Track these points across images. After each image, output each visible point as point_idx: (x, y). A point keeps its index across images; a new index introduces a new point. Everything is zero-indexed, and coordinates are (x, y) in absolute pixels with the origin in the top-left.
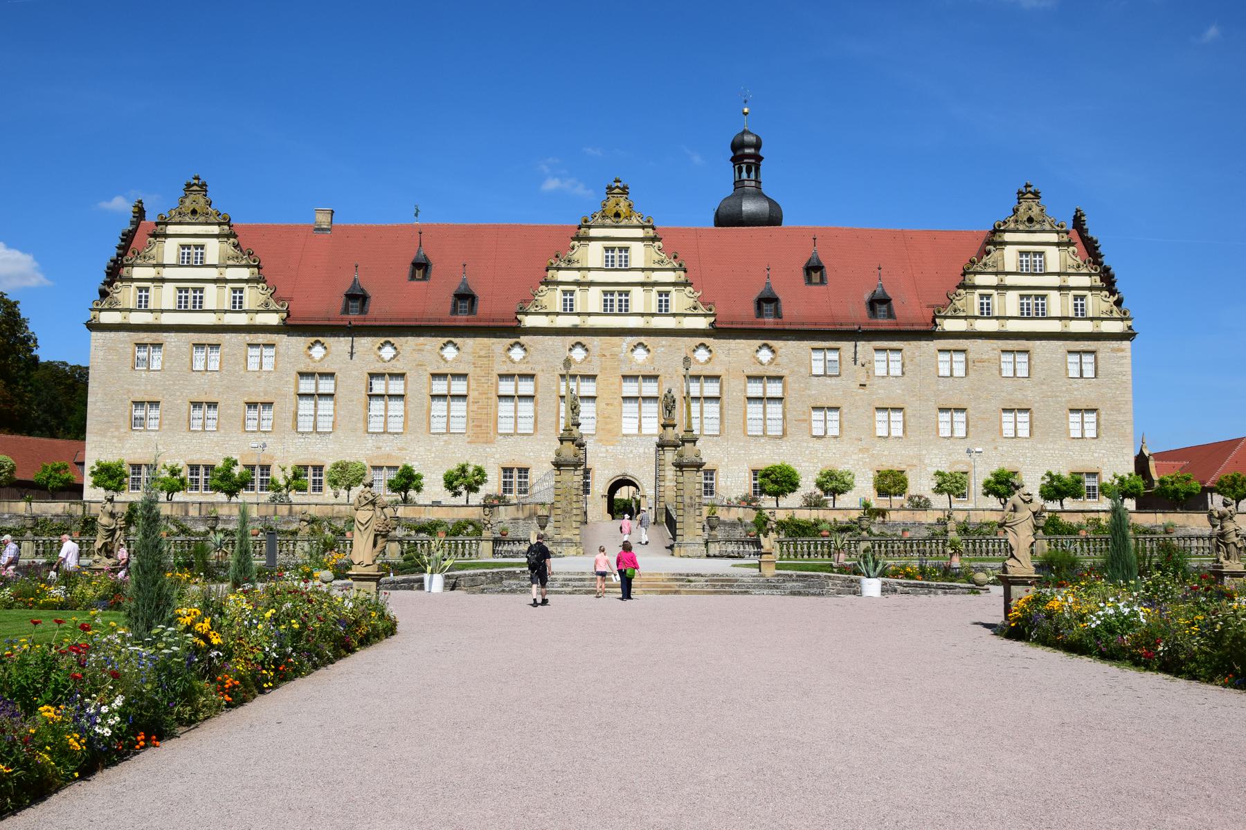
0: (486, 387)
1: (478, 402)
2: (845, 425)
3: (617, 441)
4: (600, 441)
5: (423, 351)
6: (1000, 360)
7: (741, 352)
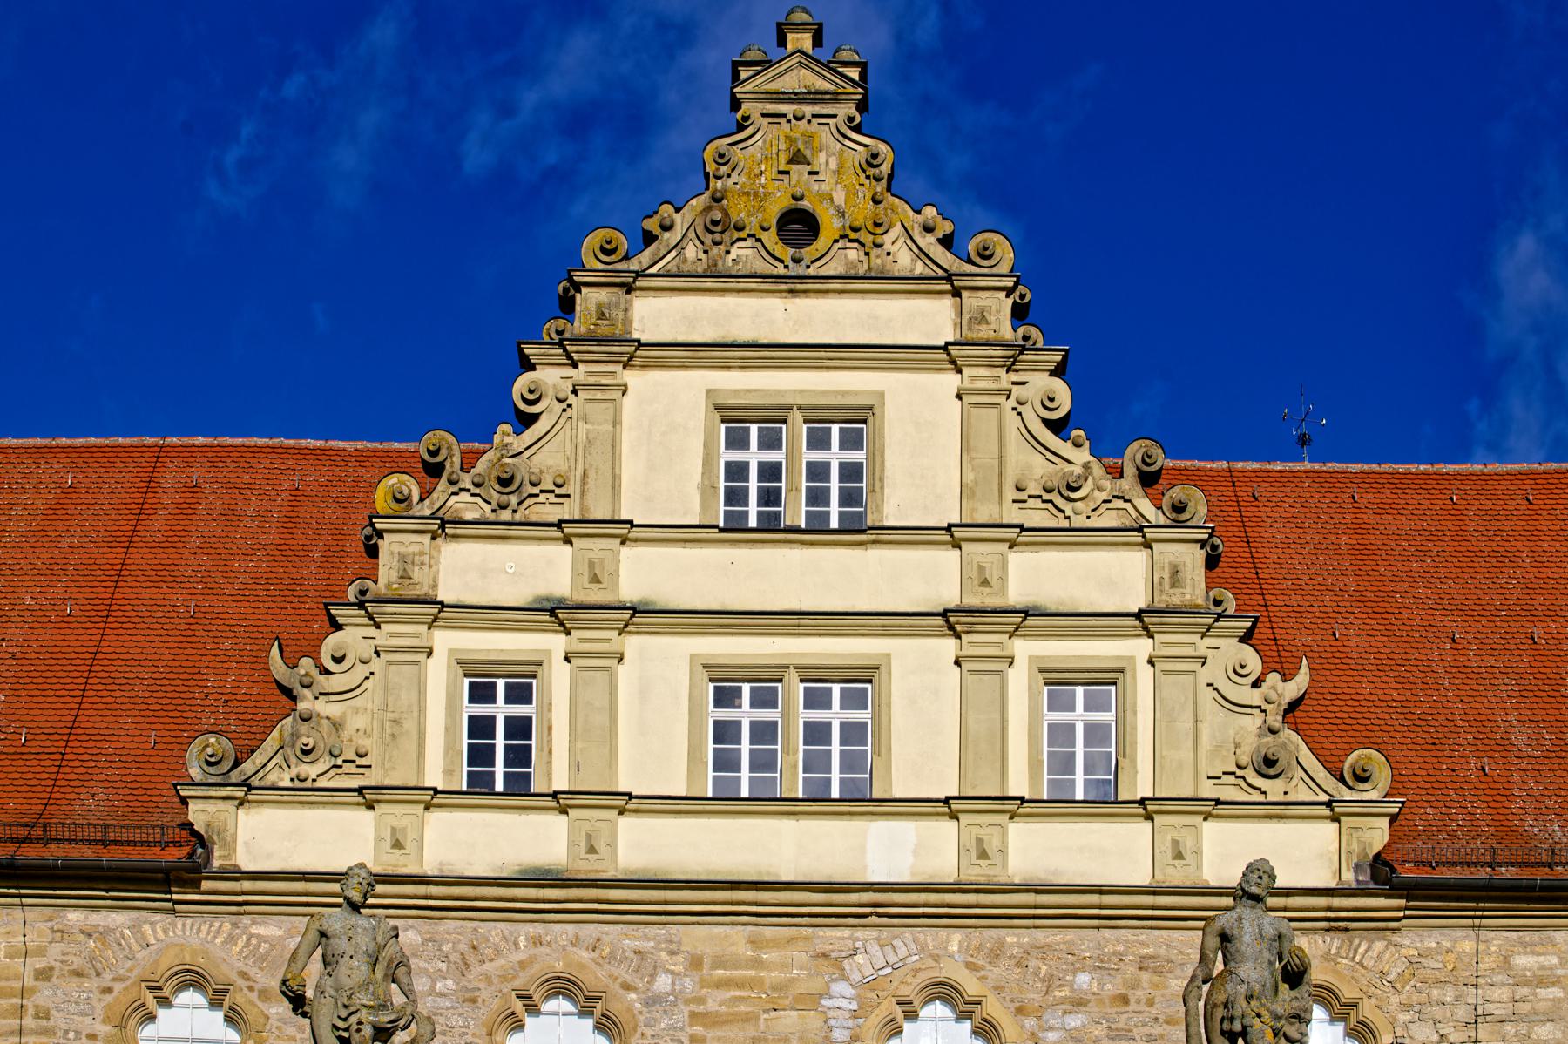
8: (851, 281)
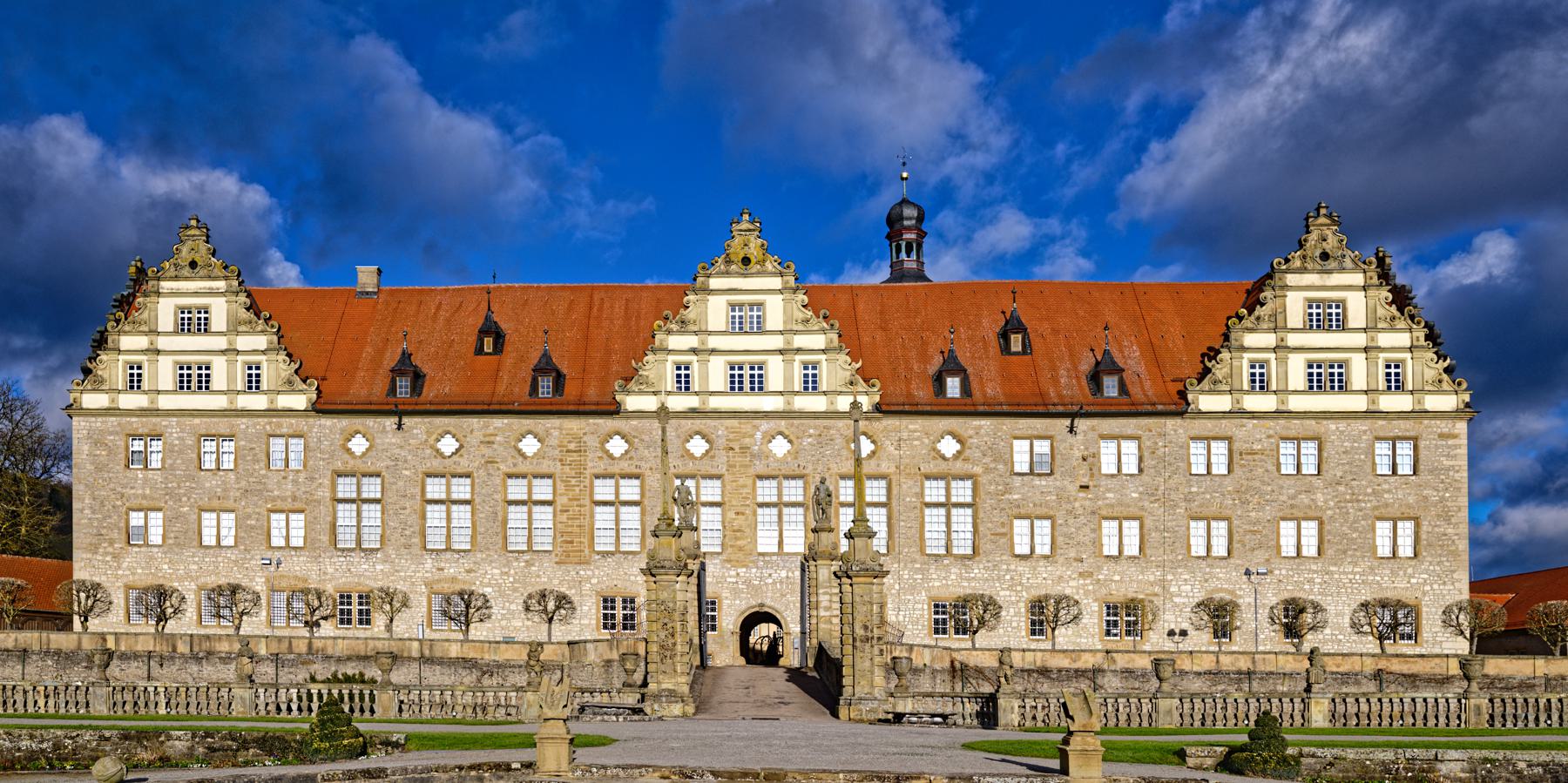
0: (577, 491)
1: (567, 511)
2: (1060, 540)
3: (753, 562)
4: (729, 561)
5: (493, 443)
6: (1278, 452)
7: (916, 443)
8: (759, 274)
